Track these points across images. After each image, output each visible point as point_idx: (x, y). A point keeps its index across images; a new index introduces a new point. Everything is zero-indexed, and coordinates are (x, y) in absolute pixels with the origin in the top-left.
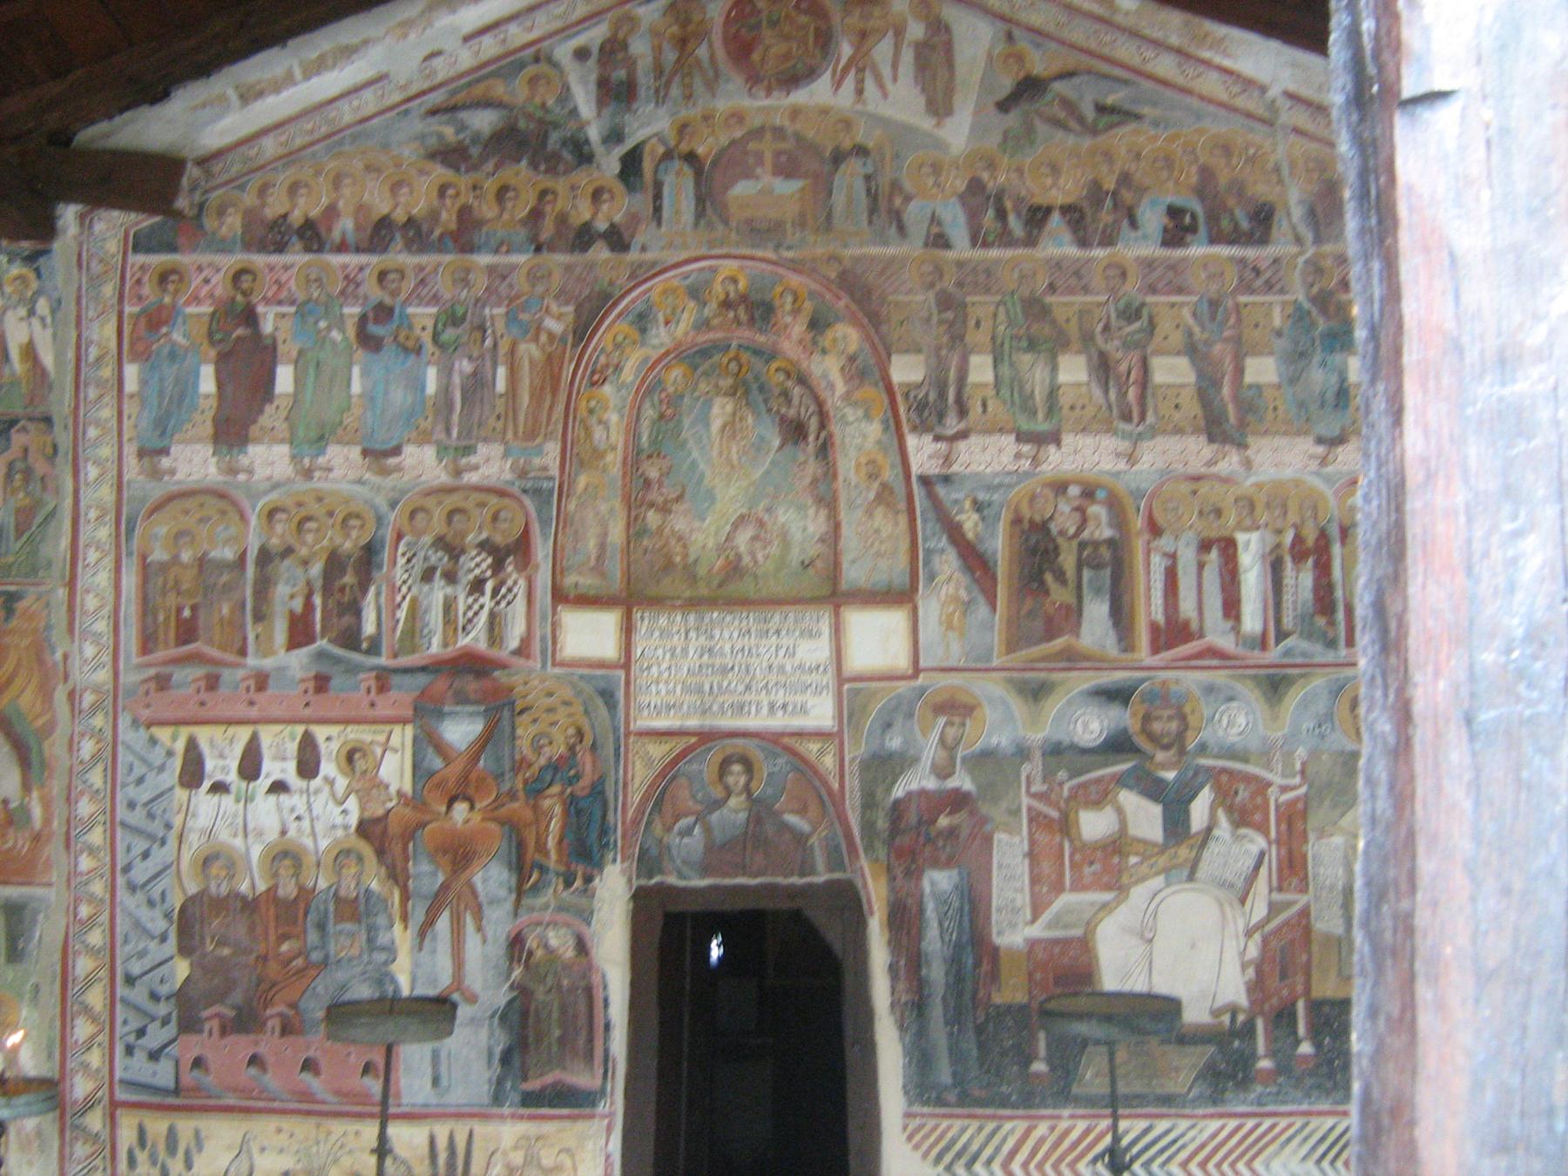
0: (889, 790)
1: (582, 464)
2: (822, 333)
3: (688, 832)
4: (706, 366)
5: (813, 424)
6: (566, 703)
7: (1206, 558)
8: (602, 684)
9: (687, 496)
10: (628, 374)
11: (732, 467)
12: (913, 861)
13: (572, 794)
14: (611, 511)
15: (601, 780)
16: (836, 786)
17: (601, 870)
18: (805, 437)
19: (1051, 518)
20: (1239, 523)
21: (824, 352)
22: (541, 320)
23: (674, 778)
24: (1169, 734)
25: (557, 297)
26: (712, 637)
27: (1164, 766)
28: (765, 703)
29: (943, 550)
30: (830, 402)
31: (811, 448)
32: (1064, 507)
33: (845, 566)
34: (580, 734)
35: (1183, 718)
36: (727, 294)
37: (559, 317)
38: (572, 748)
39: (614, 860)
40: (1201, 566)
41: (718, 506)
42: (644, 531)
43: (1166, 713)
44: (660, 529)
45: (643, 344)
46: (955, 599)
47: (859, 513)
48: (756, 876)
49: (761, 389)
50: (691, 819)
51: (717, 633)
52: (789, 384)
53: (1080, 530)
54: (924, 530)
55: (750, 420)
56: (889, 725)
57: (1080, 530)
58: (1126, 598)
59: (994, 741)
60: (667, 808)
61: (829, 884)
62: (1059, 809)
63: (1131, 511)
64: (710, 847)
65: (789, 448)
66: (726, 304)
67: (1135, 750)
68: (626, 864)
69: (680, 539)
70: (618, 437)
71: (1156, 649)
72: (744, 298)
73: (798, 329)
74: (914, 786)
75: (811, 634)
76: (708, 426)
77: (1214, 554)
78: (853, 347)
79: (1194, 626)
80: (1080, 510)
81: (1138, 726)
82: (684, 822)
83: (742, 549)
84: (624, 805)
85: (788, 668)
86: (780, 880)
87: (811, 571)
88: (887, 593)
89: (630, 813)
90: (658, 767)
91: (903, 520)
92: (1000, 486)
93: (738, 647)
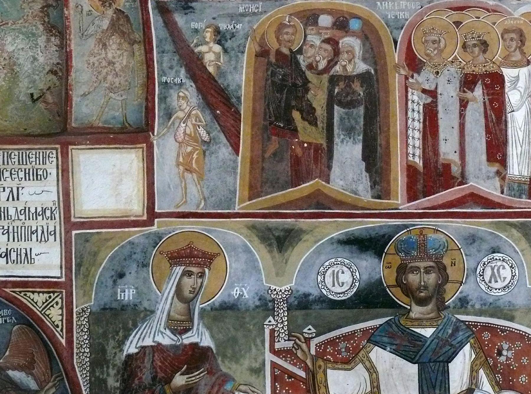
0: (121, 344)
7: (469, 95)
16: (63, 341)
19: (300, 51)
20: (506, 58)
24: (426, 288)
27: (420, 322)
29: (181, 85)
32: (315, 39)
33: (75, 100)
35: (441, 269)
40: (464, 104)
43: (422, 265)
46: (195, 138)
47: (91, 43)
53: (332, 63)
54: (160, 63)
56: (121, 275)
57: (332, 63)
58: (381, 140)
59: (235, 293)
62: (306, 369)
63: (388, 46)
67: (391, 304)
71: (412, 196)
74: (148, 342)
77: (479, 91)
79: (455, 170)
80: (332, 42)
81: (392, 281)
85: (12, 212)
87: (41, 105)
92: (243, 15)
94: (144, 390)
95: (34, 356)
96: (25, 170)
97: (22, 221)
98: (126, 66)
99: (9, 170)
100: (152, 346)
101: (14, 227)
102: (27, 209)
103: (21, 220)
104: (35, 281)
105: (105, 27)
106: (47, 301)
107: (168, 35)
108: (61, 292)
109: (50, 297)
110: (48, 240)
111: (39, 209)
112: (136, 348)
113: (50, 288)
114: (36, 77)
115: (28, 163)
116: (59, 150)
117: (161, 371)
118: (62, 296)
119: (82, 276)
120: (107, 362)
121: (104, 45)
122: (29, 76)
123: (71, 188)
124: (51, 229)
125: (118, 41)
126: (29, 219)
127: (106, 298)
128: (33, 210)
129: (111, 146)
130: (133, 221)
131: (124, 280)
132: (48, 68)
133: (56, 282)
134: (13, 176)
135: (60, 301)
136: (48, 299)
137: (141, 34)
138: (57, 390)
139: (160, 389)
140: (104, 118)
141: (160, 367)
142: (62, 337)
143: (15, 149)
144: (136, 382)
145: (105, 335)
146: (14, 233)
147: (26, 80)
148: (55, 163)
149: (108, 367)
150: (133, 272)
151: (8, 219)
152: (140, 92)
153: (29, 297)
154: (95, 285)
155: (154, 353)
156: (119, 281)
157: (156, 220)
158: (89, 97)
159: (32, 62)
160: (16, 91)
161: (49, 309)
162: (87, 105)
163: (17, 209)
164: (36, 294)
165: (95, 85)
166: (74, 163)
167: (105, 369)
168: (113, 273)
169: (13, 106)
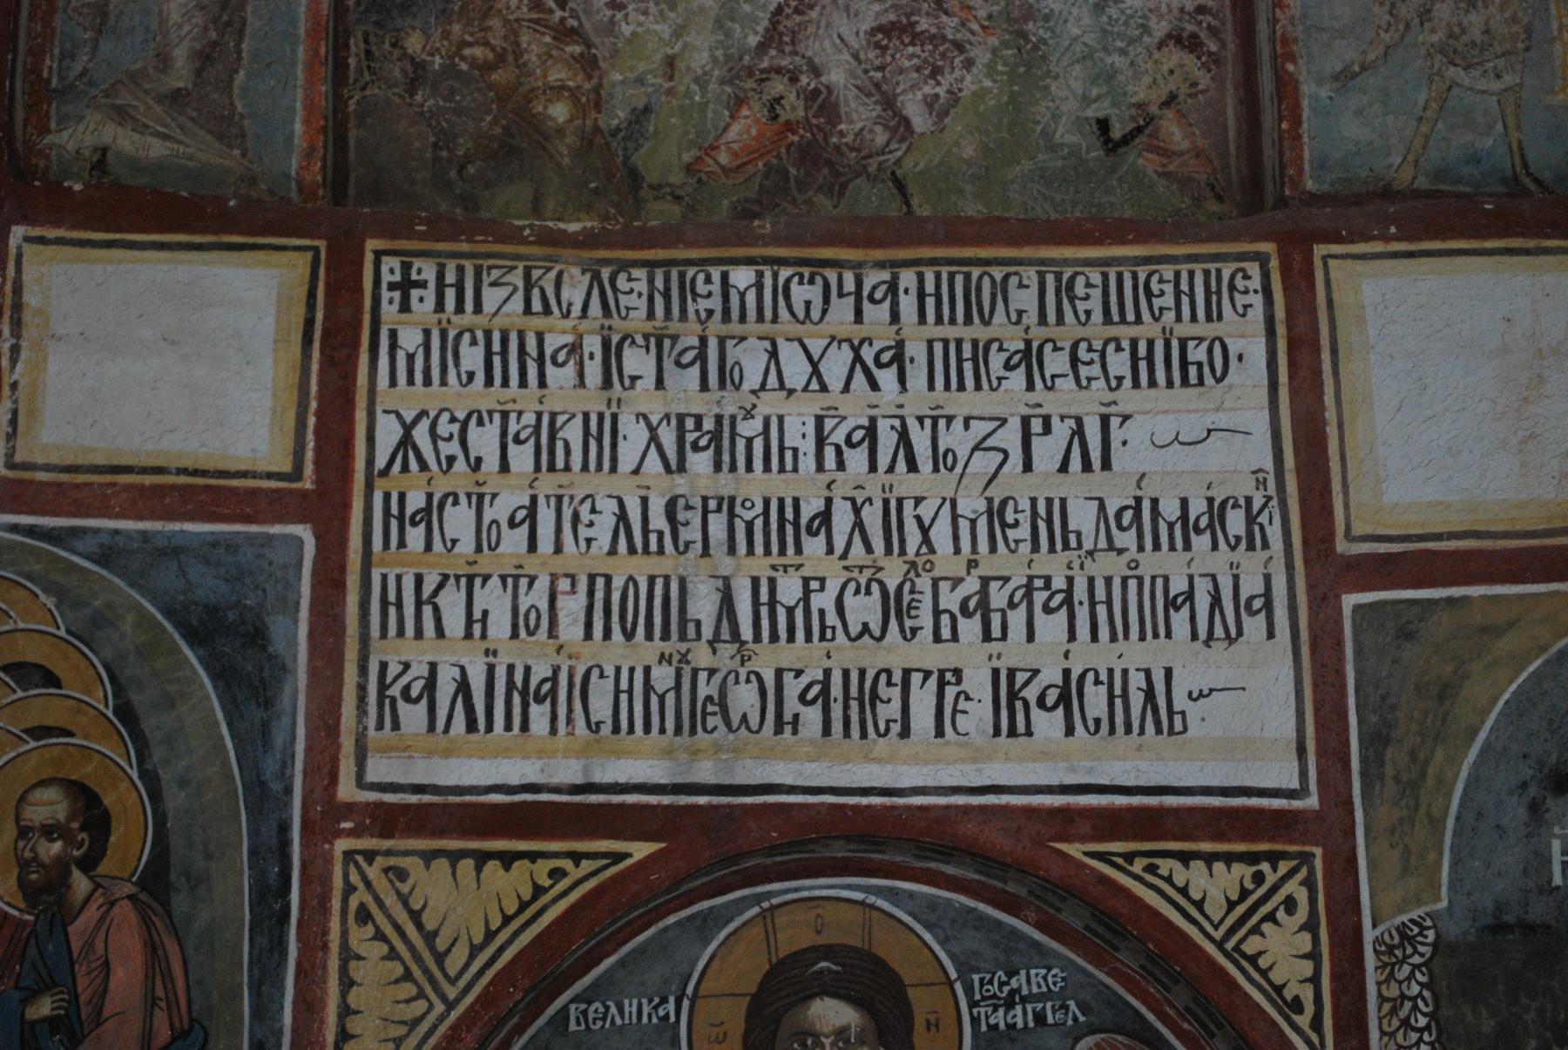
8: (208, 585)
26: (728, 377)
28: (978, 682)
33: (1311, 91)
51: (751, 358)
83: (836, 76)
85: (1082, 518)
87: (1143, 161)
88: (1514, 186)
93: (854, 410)
96: (1134, 344)
97: (1126, 557)
99: (1067, 345)
101: (1091, 580)
102: (1146, 505)
103: (1121, 551)
104: (1191, 810)
106: (1245, 893)
108: (1306, 858)
109: (1259, 878)
110: (1240, 633)
111: (1197, 507)
114: (1118, 61)
115: (1146, 316)
116: (1274, 263)
118: (1312, 872)
119: (1391, 788)
122: (1087, 57)
123: (1330, 415)
124: (1251, 585)
126: (1157, 546)
128: (1170, 510)
129: (1489, 244)
132: (1160, 28)
134: (1084, 371)
135: (1302, 895)
136: (1249, 885)
143: (1088, 263)
146: (1093, 604)
147: (1077, 70)
148: (1257, 313)
151: (1066, 546)
153: (1169, 880)
154: (1450, 823)
160: (1042, 110)
161: (1256, 930)
162: (1359, 113)
163: (1102, 507)
166: (1338, 314)
169: (1027, 165)
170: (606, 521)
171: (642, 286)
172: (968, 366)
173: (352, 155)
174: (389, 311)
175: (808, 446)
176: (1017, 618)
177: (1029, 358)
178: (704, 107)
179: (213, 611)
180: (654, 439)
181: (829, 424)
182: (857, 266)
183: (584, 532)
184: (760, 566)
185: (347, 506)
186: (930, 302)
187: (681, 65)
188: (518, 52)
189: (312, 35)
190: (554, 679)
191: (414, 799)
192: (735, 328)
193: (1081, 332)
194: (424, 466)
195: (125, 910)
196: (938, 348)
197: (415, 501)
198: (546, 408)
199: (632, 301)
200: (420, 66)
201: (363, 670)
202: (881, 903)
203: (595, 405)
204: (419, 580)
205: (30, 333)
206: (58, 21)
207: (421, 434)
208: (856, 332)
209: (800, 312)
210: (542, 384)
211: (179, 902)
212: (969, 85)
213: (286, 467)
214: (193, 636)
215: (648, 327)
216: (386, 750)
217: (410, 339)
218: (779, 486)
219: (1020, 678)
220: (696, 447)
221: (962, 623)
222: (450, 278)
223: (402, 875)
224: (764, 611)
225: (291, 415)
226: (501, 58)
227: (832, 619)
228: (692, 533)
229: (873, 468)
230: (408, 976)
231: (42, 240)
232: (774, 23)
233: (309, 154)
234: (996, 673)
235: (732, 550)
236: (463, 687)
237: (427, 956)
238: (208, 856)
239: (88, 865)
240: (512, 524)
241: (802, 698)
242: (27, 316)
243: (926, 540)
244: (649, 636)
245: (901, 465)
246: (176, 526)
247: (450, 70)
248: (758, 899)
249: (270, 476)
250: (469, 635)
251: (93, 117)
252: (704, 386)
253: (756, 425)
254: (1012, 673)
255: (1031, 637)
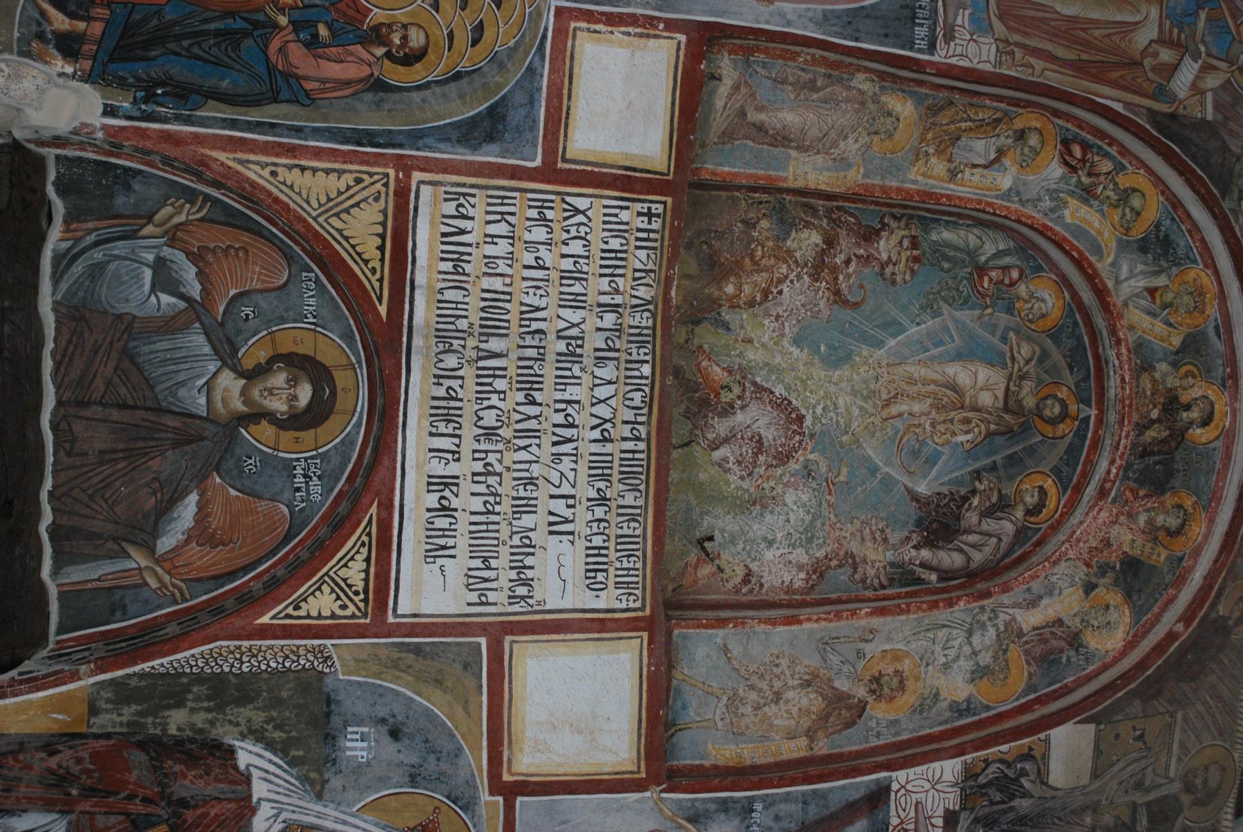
0: (257, 735)
1: (934, 110)
2: (1116, 583)
3: (164, 279)
4: (1056, 356)
5: (951, 559)
6: (479, 31)
8: (516, 116)
9: (846, 314)
10: (1076, 213)
11: (887, 403)
12: (88, 792)
13: (275, 26)
14: (843, 163)
15: (305, 99)
16: (265, 619)
17: (87, 78)
18: (928, 543)
21: (1089, 588)
22: (1196, 56)
23: (290, 258)
25: (1226, 85)
28: (453, 469)
30: (1006, 599)
31: (909, 554)
33: (720, 634)
34: (411, 58)
36: (1188, 407)
37: (1196, 89)
38: (378, 35)
39: (109, 111)
41: (819, 373)
42: (786, 224)
44: (786, 256)
45: (1123, 246)
47: (813, 661)
48: (55, 427)
49: (1012, 460)
50: (194, 289)
51: (607, 372)
52: (1019, 513)
54: (787, 798)
55: (961, 438)
56: (395, 734)
60: (220, 238)
61: (42, 589)
64: (128, 326)
65: (912, 510)
66: (1172, 405)
68: (100, 135)
69: (766, 293)
70: (970, 186)
72: (1179, 436)
73: (1126, 538)
74: (259, 789)
75: (593, 571)
76: (959, 357)
78: (1092, 641)
82: (189, 273)
83: (740, 417)
84: (242, 144)
85: (527, 521)
86: (48, 484)
87: (694, 555)
89: (222, 156)
90: (328, 227)
91: (796, 749)
94: (159, 784)
95: (225, 545)
96: (606, 548)
97: (508, 540)
98: (771, 725)
99: (607, 518)
100: (250, 796)
101: (498, 523)
102: (532, 550)
103: (511, 537)
104: (390, 564)
105: (837, 684)
106: (350, 586)
107: (833, 809)
108: (365, 615)
109: (357, 593)
110: (471, 590)
111: (530, 574)
112: (248, 766)
113: (375, 592)
114: (740, 547)
115: (619, 554)
116: (640, 614)
117: (199, 817)
118: (358, 618)
119: (397, 655)
120: (220, 708)
121: (808, 684)
122: (743, 532)
123: (569, 636)
124: (492, 596)
125: (814, 709)
126: (512, 554)
127: (352, 704)
128: (529, 561)
129: (644, 712)
130: (500, 754)
131: (386, 740)
132: (754, 567)
133: (386, 604)
134: (595, 525)
135: (348, 612)
136: (354, 589)
137: (825, 751)
138: (154, 591)
139: (159, 816)
140: (686, 688)
141: (205, 815)
142: (273, 617)
143: (645, 529)
144: (177, 768)
145: (278, 702)
146: (487, 523)
148: (618, 605)
149: (208, 710)
150: (401, 756)
151: (514, 513)
152: (728, 754)
153: (358, 552)
154: (378, 682)
155: (237, 801)
156: (384, 729)
157: (500, 799)
158: (723, 660)
159: (765, 539)
160: (719, 510)
161: (333, 591)
163: (531, 530)
164: (364, 565)
165: (743, 669)
167: (205, 704)
168: (400, 718)
169: (694, 503)
170: (536, 301)
171: (644, 324)
172: (600, 471)
173: (714, 193)
174: (638, 207)
175: (566, 396)
176: (482, 488)
177: (602, 500)
178: (729, 355)
179: (503, 118)
180: (573, 325)
181: (576, 406)
182: (649, 423)
183: (531, 291)
184: (512, 371)
185: (549, 183)
186: (630, 456)
187: (748, 346)
188: (758, 271)
189: (768, 178)
190: (464, 274)
191: (412, 206)
192: (623, 365)
193: (613, 524)
194: (566, 219)
195: (366, 71)
196: (609, 458)
197: (550, 214)
198: (590, 277)
199: (638, 318)
200: (754, 226)
201: (472, 186)
202: (355, 419)
203: (591, 299)
204: (513, 214)
205: (636, 41)
206: (780, 61)
207: (580, 218)
208: (618, 421)
209: (629, 396)
210: (601, 275)
211: (369, 96)
212: (732, 478)
213: (568, 156)
214: (492, 109)
215: (625, 326)
216: (435, 195)
217: (625, 216)
218: (549, 382)
219: (454, 489)
220: (568, 344)
221: (481, 463)
222: (652, 236)
223: (377, 199)
224: (491, 372)
225: (592, 159)
226: (756, 263)
227: (486, 403)
228: (529, 341)
229: (555, 426)
230: (329, 200)
231: (678, 49)
232: (765, 390)
233: (714, 173)
234: (457, 477)
235: (520, 359)
236: (462, 232)
237: (339, 209)
238: (390, 111)
239: (388, 55)
240: (537, 258)
241: (450, 388)
242: (644, 40)
243: (520, 448)
244: (482, 319)
245: (555, 439)
246: (543, 104)
247: (751, 240)
248: (359, 362)
249: (565, 148)
250: (486, 235)
251: (736, 75)
252: (596, 350)
253: (577, 372)
254: (457, 485)
255: (473, 494)
